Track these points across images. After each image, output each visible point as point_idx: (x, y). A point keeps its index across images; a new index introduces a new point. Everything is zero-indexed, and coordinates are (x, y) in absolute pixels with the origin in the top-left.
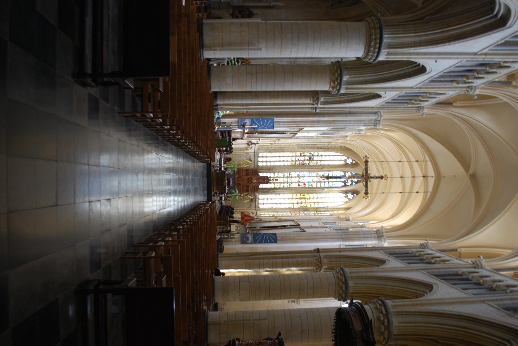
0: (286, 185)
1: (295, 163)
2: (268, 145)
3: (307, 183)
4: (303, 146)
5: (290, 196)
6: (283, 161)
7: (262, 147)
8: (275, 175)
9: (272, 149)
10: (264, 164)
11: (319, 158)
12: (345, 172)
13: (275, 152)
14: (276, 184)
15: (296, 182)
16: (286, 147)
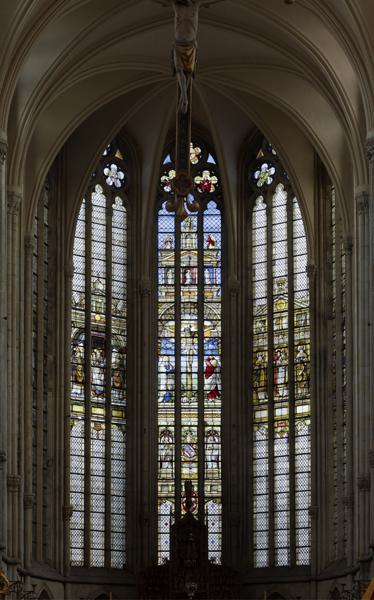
0: (213, 452)
1: (117, 408)
2: (34, 523)
3: (206, 358)
4: (41, 366)
5: (261, 434)
6: (107, 459)
7: (40, 547)
8: (167, 498)
9: (49, 501)
10: (117, 542)
11: (98, 302)
12: (161, 196)
13: (65, 490)
14: (207, 494)
15: (201, 409)
16: (45, 443)
